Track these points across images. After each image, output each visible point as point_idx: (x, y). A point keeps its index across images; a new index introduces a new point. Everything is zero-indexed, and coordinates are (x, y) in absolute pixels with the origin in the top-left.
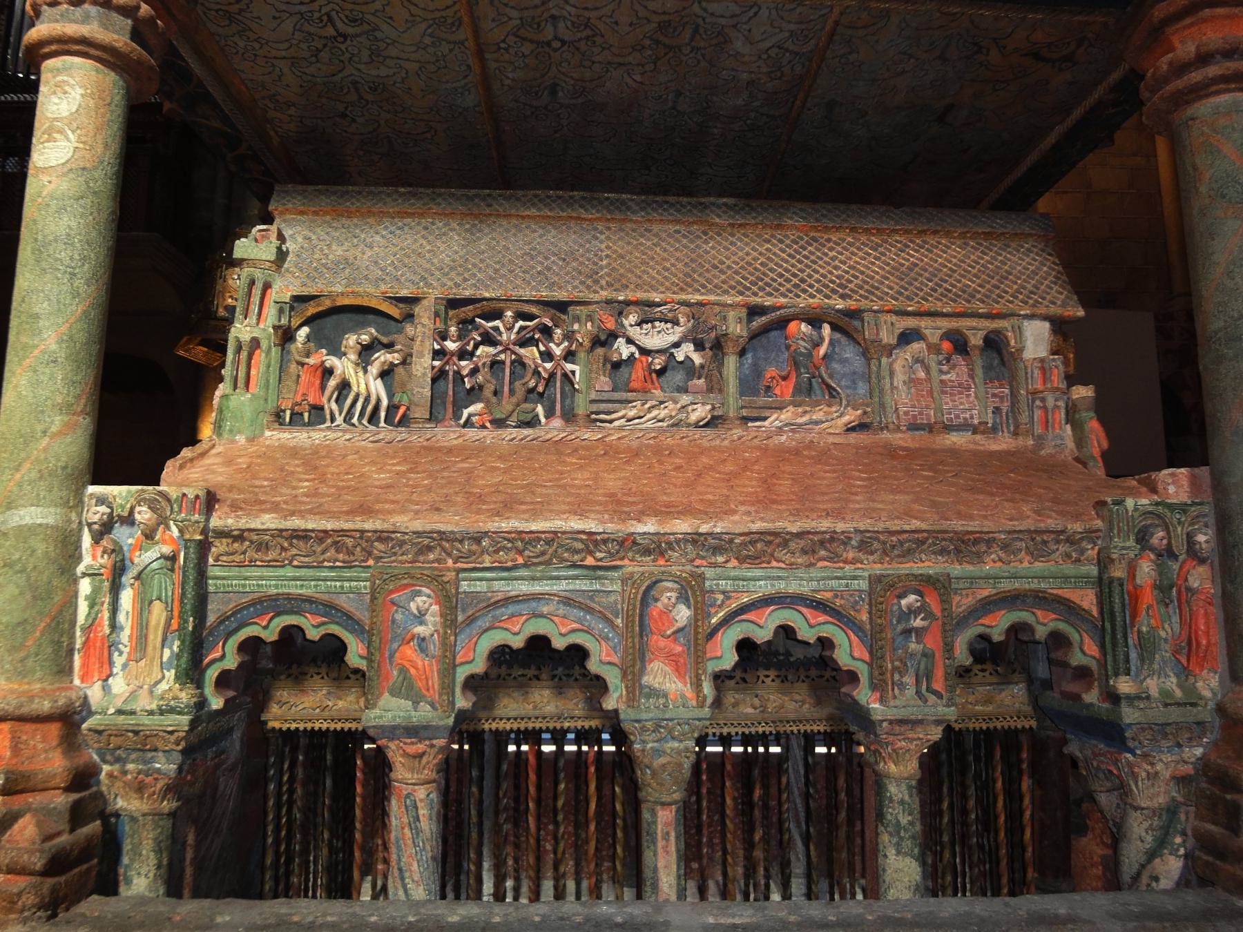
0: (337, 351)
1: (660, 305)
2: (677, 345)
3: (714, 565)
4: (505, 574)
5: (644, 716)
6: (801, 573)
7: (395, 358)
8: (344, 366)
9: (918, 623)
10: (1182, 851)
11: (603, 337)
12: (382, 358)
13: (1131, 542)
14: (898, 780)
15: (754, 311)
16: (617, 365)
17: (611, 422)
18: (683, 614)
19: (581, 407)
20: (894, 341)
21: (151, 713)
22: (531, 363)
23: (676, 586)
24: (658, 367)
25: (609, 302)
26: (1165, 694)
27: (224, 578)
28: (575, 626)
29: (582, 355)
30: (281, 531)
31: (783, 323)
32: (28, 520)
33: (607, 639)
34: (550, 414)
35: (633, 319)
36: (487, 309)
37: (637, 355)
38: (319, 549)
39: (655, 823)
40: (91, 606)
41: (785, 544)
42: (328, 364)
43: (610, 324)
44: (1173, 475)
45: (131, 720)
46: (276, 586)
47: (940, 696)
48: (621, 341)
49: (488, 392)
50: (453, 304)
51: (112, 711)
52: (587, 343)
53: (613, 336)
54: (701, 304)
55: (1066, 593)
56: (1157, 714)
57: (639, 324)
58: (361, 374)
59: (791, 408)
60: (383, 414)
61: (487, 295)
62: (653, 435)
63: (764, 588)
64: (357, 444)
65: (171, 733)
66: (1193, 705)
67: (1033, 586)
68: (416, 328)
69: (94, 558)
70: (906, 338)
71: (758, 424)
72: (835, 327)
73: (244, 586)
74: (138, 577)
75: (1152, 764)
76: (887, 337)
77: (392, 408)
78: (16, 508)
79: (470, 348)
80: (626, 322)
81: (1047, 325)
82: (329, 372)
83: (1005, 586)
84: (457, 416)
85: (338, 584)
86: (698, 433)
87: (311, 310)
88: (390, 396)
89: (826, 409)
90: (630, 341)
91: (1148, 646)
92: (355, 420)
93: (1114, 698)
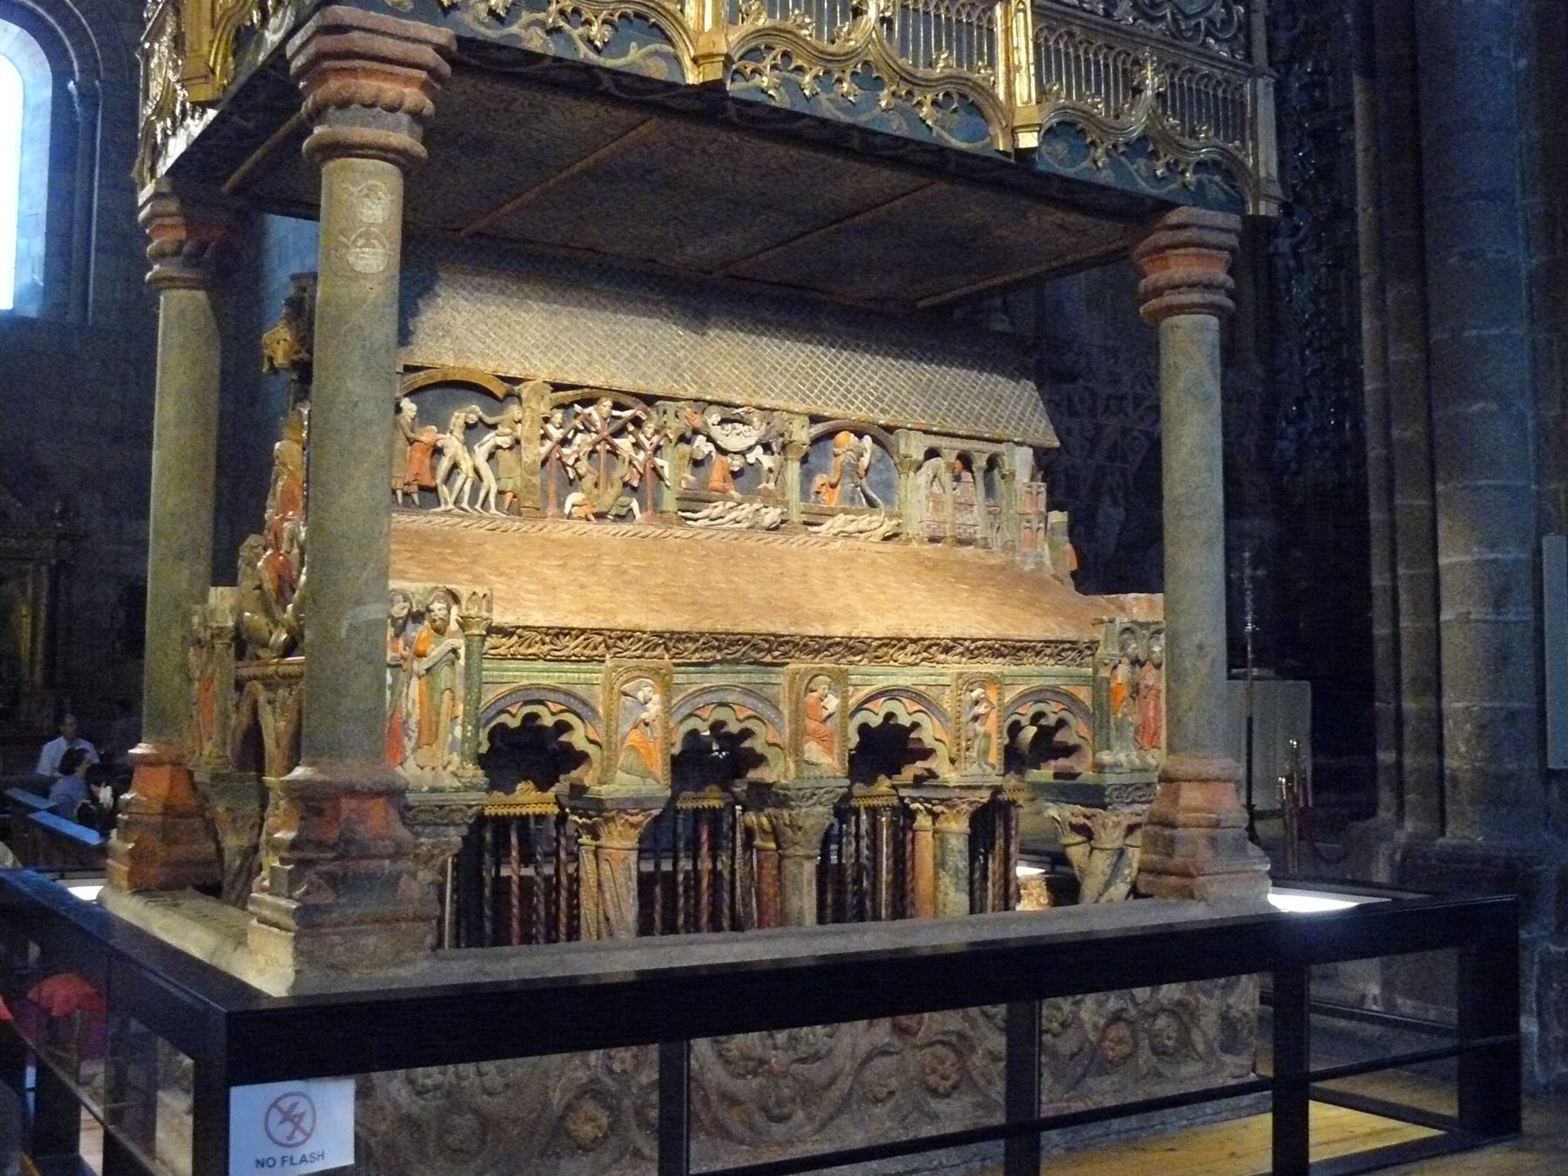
0: (443, 428)
1: (738, 407)
2: (751, 449)
3: (851, 663)
4: (700, 669)
5: (806, 785)
6: (908, 670)
7: (505, 441)
8: (453, 443)
9: (981, 709)
10: (1129, 880)
11: (688, 434)
12: (490, 439)
13: (1117, 652)
14: (958, 834)
15: (815, 419)
16: (697, 463)
17: (696, 520)
18: (832, 703)
19: (669, 503)
20: (921, 458)
21: (457, 790)
22: (626, 456)
23: (829, 680)
24: (736, 469)
25: (696, 400)
26: (1131, 763)
27: (487, 670)
28: (750, 713)
29: (668, 450)
30: (549, 628)
31: (830, 435)
32: (373, 616)
33: (773, 724)
34: (642, 507)
35: (716, 418)
36: (587, 397)
37: (714, 454)
38: (573, 644)
39: (802, 874)
40: (392, 695)
41: (903, 648)
42: (439, 444)
43: (697, 422)
44: (1137, 599)
45: (442, 797)
46: (528, 677)
47: (993, 767)
48: (700, 440)
49: (588, 483)
50: (557, 387)
51: (426, 789)
52: (674, 441)
53: (696, 432)
54: (773, 410)
55: (1071, 689)
56: (1125, 779)
57: (720, 423)
58: (467, 455)
59: (841, 515)
60: (492, 498)
61: (591, 383)
62: (735, 535)
63: (882, 683)
64: (475, 531)
65: (470, 807)
66: (1146, 770)
67: (1052, 683)
68: (524, 411)
69: (395, 650)
70: (932, 453)
71: (815, 529)
72: (875, 440)
73: (502, 677)
74: (428, 670)
75: (1117, 816)
76: (918, 455)
77: (501, 493)
78: (364, 604)
79: (570, 436)
80: (710, 422)
81: (1031, 451)
82: (437, 451)
83: (1036, 683)
84: (561, 505)
85: (576, 675)
86: (772, 536)
87: (420, 378)
88: (498, 479)
89: (868, 519)
90: (710, 439)
91: (1120, 727)
92: (465, 505)
93: (1099, 768)
